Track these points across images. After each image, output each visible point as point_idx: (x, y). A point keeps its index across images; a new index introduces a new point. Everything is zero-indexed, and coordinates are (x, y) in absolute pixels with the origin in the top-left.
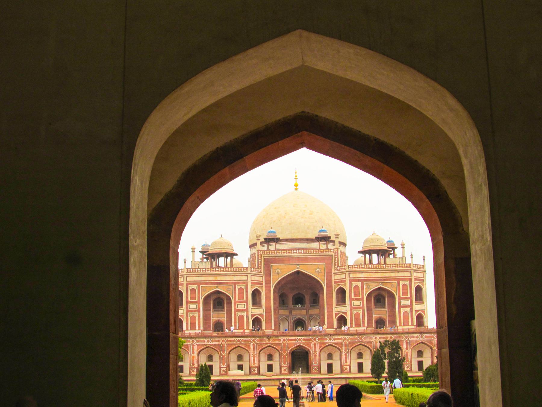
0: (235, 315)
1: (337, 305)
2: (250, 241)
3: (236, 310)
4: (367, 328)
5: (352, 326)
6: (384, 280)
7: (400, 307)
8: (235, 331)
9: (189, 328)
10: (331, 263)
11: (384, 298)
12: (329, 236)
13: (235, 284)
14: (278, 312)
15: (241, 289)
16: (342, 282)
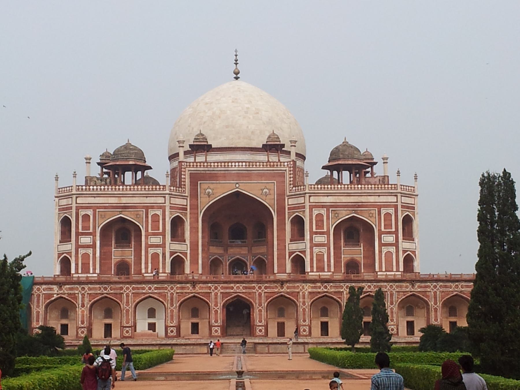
0: (147, 252)
1: (291, 241)
2: (170, 150)
3: (148, 246)
4: (333, 273)
5: (312, 271)
6: (359, 206)
7: (381, 245)
8: (145, 275)
9: (80, 271)
11: (358, 231)
12: (281, 143)
13: (147, 208)
14: (209, 249)
15: (156, 215)
16: (298, 208)
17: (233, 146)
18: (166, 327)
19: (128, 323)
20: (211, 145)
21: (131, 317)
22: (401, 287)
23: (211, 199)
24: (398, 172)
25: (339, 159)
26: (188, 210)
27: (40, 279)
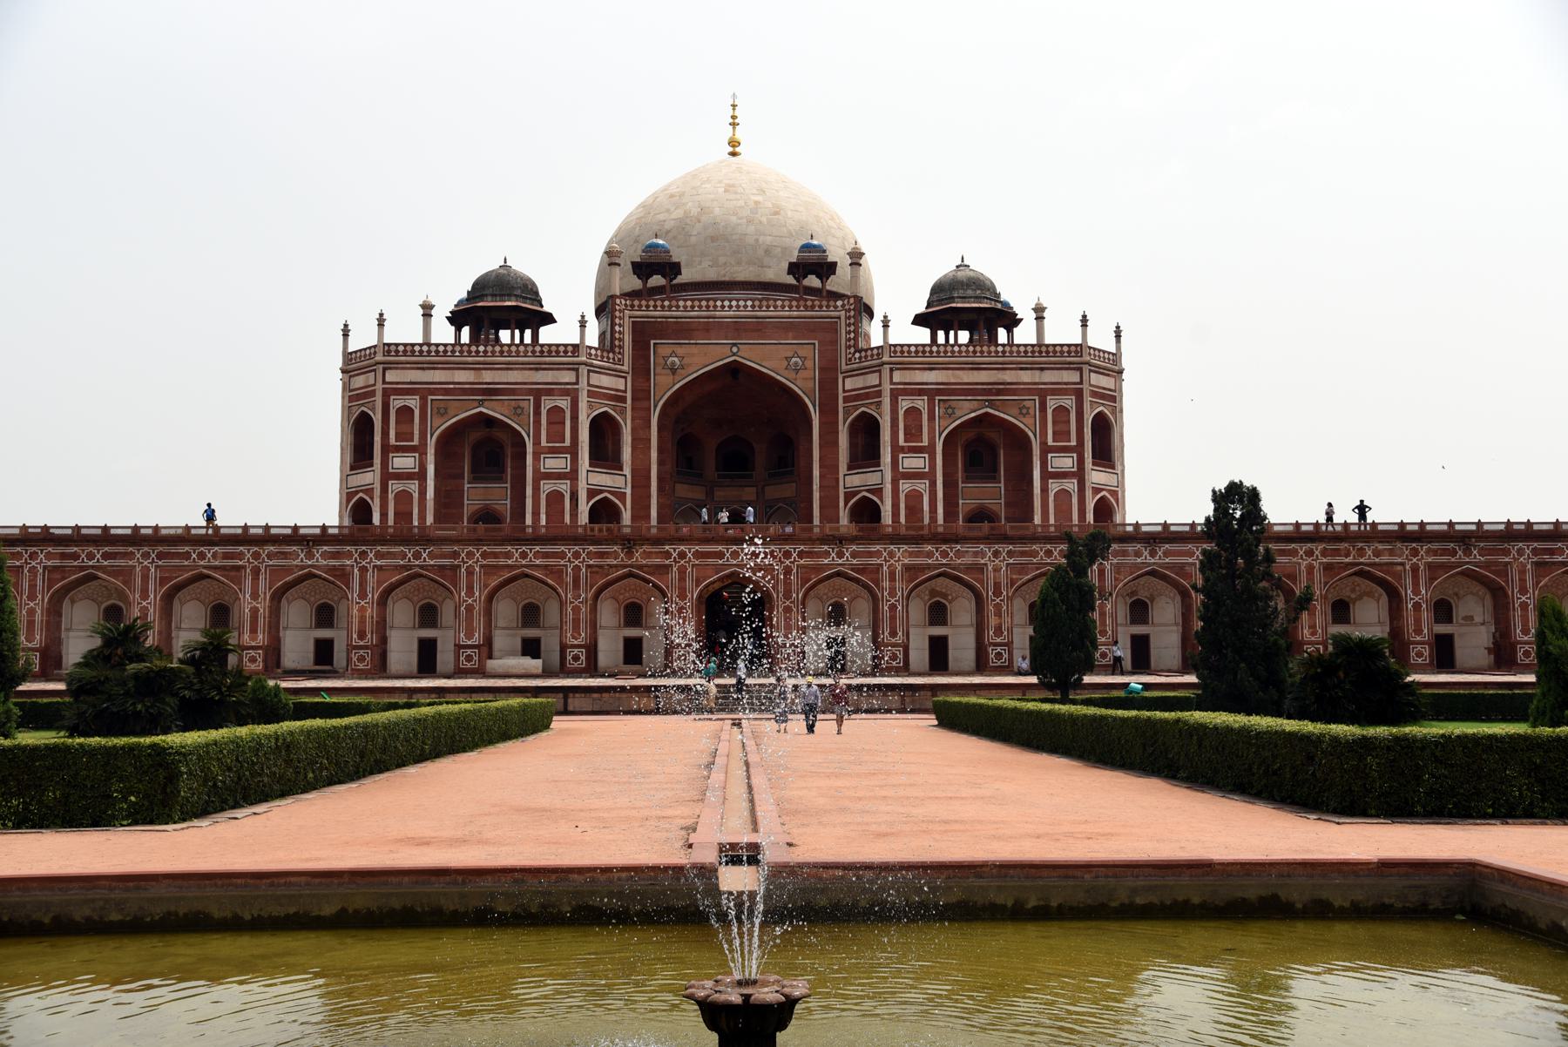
0: (536, 489)
3: (539, 476)
6: (999, 392)
7: (1046, 475)
10: (835, 342)
13: (538, 394)
15: (556, 411)
16: (867, 396)
17: (727, 279)
18: (563, 648)
19: (469, 635)
20: (675, 269)
21: (479, 623)
22: (1124, 553)
23: (677, 378)
24: (1084, 321)
25: (952, 299)
26: (629, 401)
27: (260, 531)
